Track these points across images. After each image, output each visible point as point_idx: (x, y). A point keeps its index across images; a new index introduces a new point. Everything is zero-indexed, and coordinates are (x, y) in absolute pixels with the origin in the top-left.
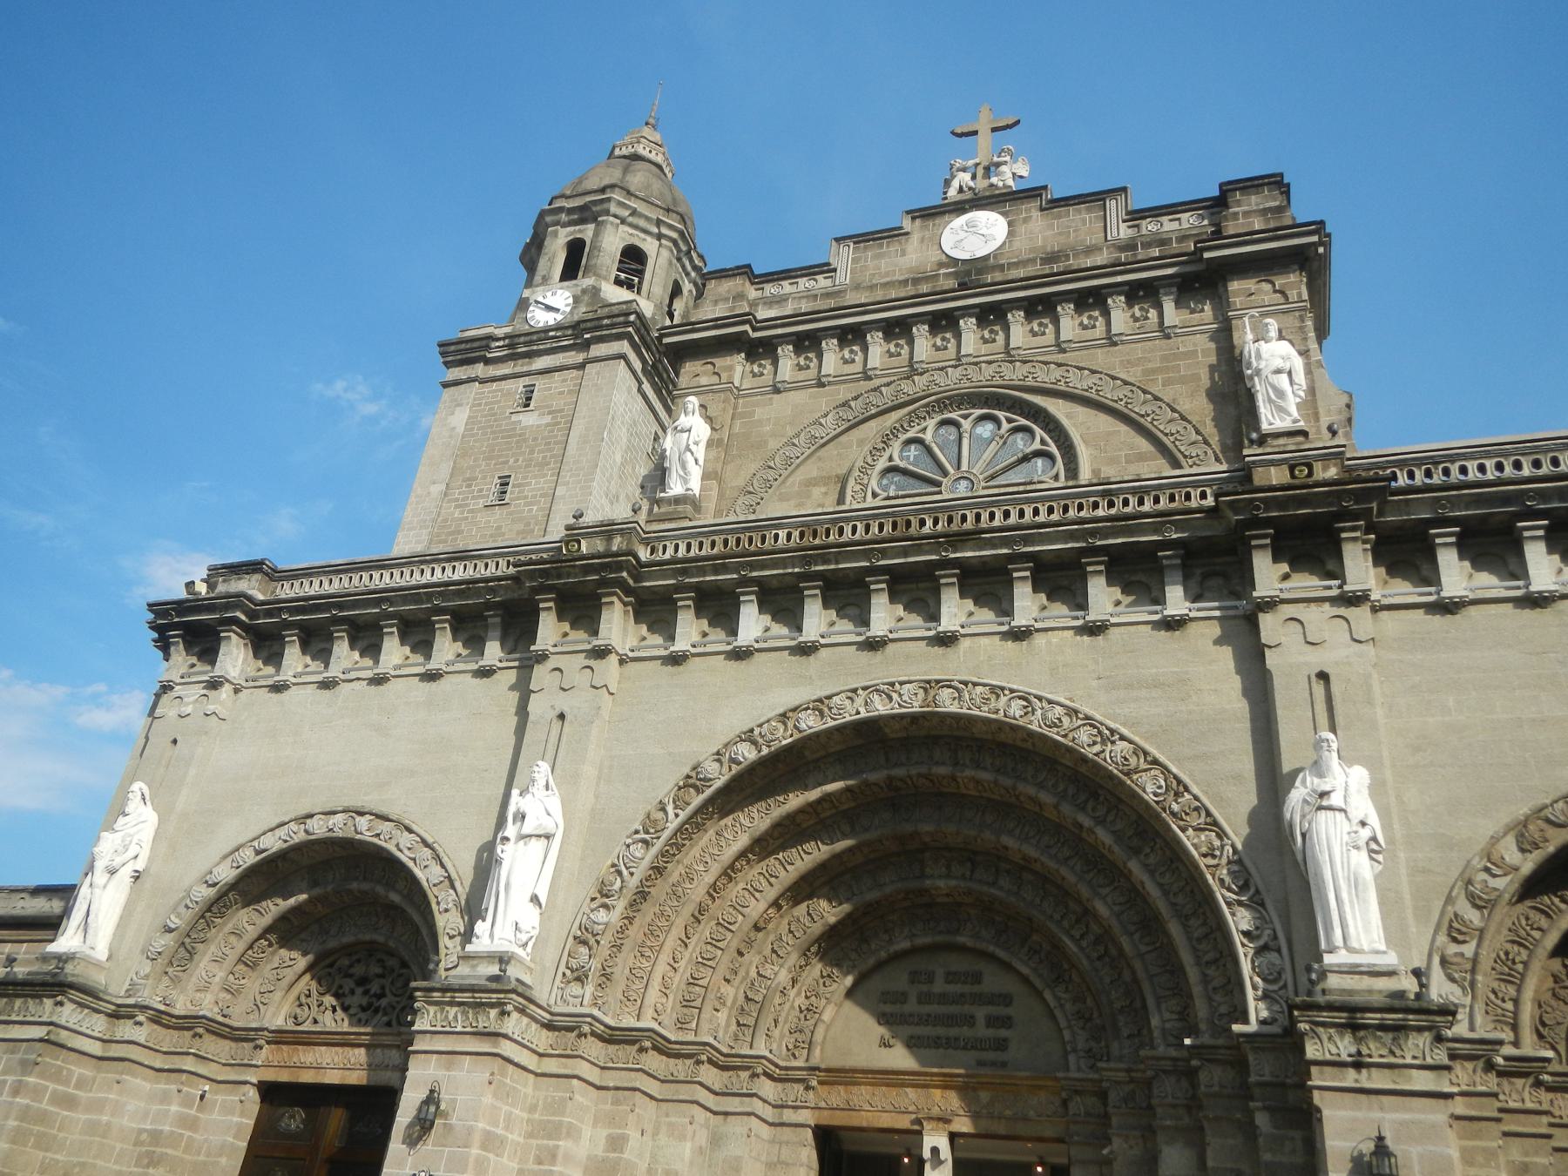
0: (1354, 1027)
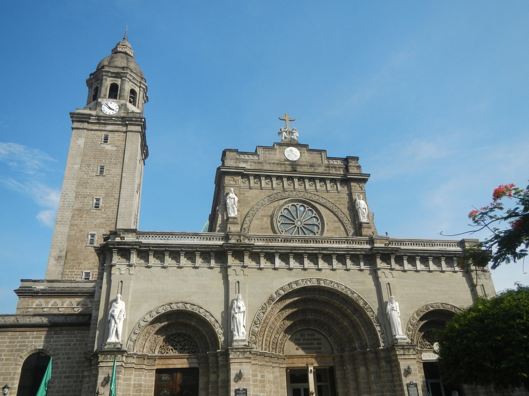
0: (403, 349)
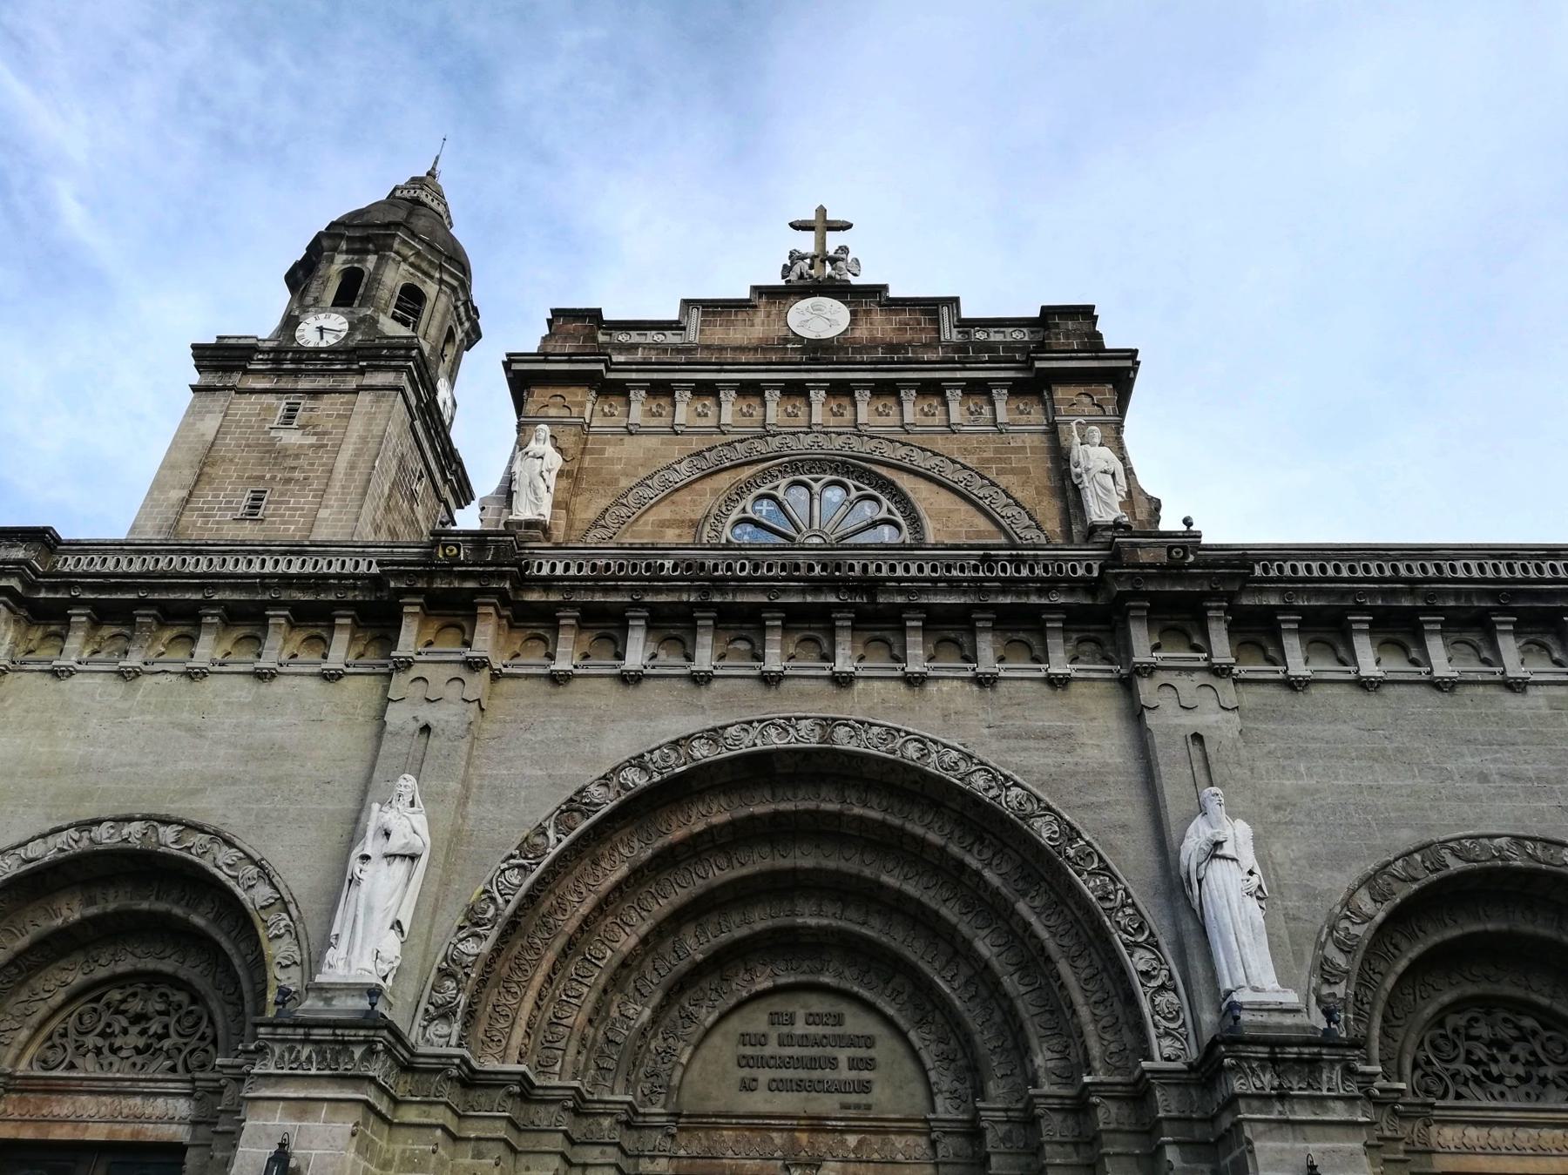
0: (1274, 1062)
